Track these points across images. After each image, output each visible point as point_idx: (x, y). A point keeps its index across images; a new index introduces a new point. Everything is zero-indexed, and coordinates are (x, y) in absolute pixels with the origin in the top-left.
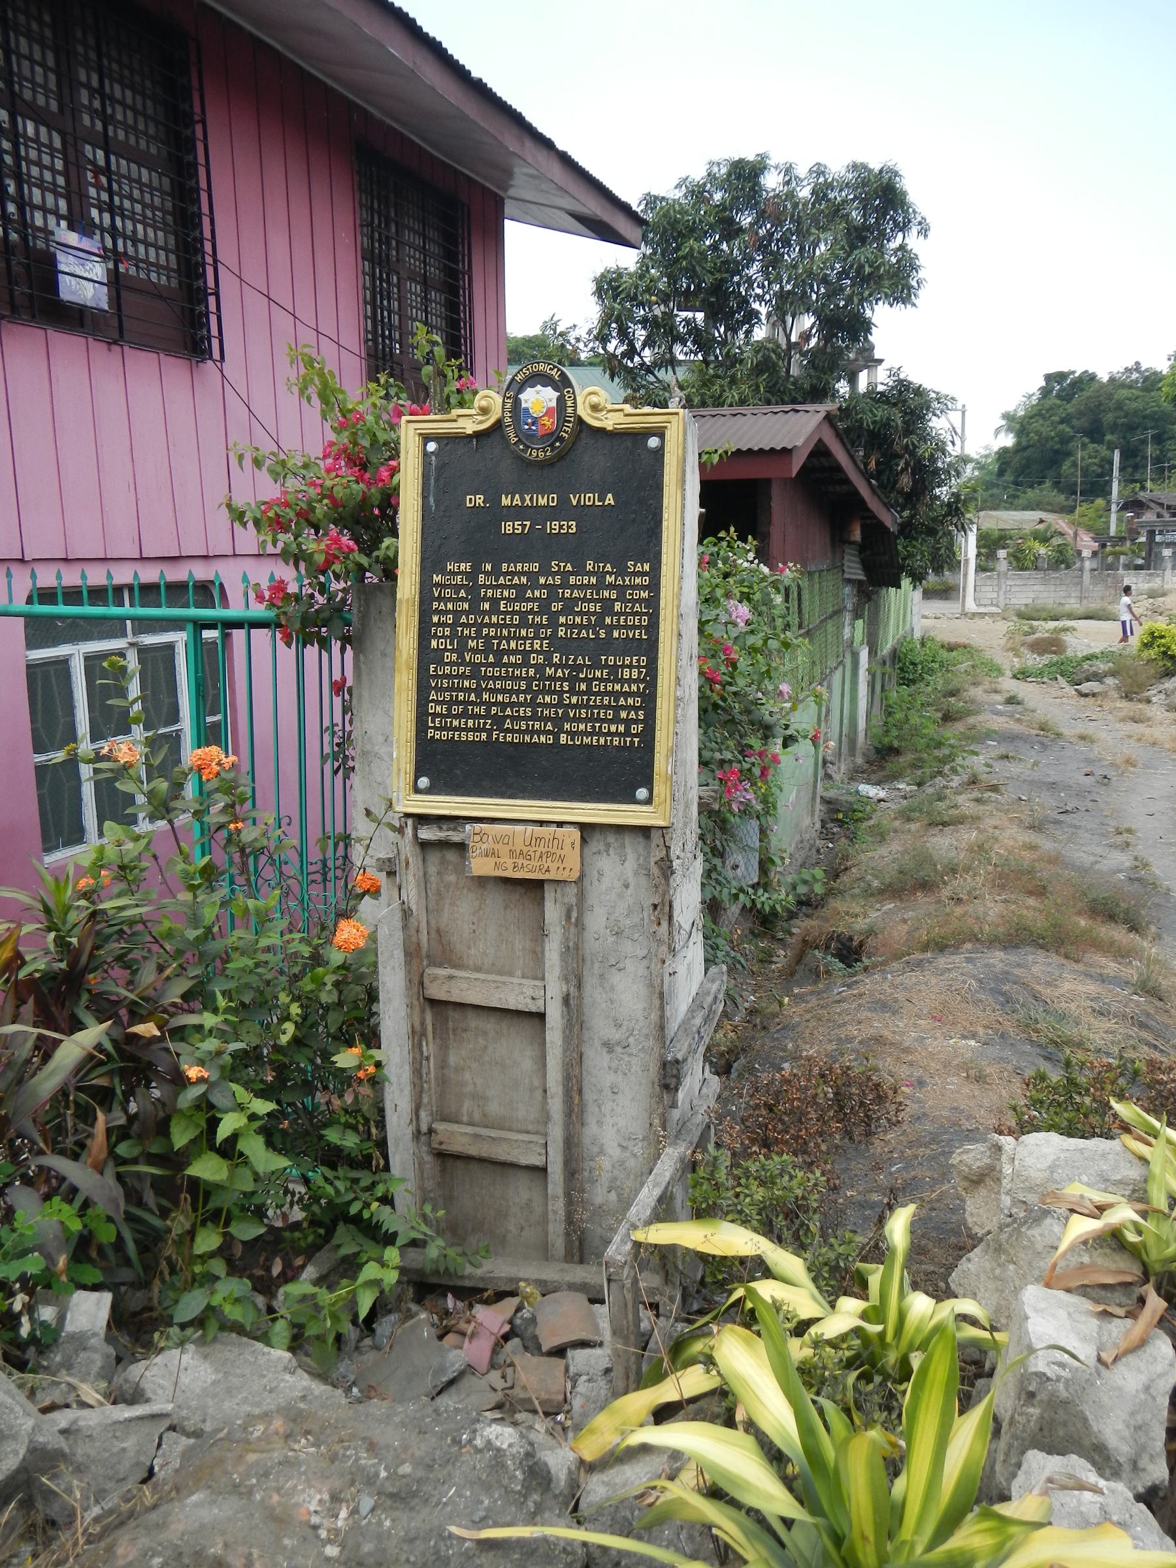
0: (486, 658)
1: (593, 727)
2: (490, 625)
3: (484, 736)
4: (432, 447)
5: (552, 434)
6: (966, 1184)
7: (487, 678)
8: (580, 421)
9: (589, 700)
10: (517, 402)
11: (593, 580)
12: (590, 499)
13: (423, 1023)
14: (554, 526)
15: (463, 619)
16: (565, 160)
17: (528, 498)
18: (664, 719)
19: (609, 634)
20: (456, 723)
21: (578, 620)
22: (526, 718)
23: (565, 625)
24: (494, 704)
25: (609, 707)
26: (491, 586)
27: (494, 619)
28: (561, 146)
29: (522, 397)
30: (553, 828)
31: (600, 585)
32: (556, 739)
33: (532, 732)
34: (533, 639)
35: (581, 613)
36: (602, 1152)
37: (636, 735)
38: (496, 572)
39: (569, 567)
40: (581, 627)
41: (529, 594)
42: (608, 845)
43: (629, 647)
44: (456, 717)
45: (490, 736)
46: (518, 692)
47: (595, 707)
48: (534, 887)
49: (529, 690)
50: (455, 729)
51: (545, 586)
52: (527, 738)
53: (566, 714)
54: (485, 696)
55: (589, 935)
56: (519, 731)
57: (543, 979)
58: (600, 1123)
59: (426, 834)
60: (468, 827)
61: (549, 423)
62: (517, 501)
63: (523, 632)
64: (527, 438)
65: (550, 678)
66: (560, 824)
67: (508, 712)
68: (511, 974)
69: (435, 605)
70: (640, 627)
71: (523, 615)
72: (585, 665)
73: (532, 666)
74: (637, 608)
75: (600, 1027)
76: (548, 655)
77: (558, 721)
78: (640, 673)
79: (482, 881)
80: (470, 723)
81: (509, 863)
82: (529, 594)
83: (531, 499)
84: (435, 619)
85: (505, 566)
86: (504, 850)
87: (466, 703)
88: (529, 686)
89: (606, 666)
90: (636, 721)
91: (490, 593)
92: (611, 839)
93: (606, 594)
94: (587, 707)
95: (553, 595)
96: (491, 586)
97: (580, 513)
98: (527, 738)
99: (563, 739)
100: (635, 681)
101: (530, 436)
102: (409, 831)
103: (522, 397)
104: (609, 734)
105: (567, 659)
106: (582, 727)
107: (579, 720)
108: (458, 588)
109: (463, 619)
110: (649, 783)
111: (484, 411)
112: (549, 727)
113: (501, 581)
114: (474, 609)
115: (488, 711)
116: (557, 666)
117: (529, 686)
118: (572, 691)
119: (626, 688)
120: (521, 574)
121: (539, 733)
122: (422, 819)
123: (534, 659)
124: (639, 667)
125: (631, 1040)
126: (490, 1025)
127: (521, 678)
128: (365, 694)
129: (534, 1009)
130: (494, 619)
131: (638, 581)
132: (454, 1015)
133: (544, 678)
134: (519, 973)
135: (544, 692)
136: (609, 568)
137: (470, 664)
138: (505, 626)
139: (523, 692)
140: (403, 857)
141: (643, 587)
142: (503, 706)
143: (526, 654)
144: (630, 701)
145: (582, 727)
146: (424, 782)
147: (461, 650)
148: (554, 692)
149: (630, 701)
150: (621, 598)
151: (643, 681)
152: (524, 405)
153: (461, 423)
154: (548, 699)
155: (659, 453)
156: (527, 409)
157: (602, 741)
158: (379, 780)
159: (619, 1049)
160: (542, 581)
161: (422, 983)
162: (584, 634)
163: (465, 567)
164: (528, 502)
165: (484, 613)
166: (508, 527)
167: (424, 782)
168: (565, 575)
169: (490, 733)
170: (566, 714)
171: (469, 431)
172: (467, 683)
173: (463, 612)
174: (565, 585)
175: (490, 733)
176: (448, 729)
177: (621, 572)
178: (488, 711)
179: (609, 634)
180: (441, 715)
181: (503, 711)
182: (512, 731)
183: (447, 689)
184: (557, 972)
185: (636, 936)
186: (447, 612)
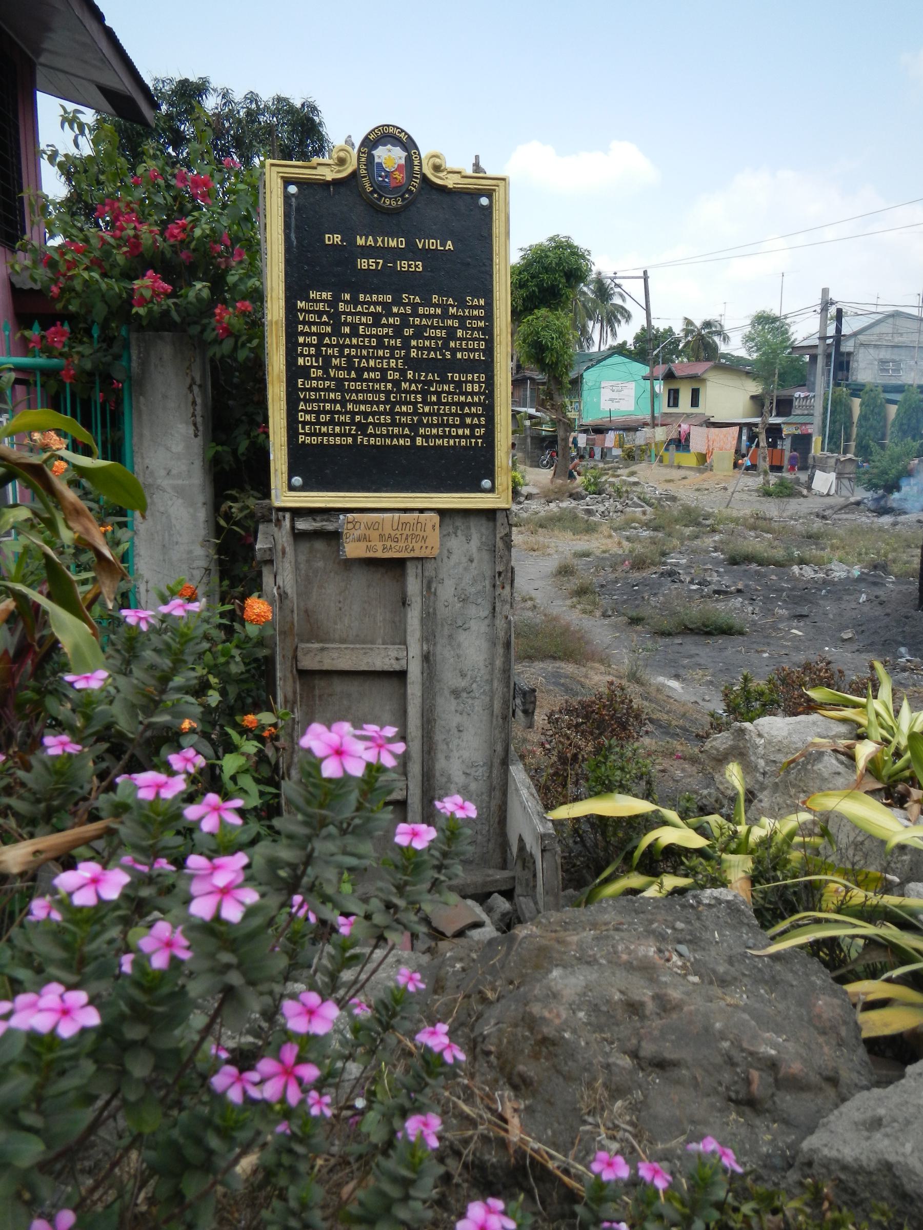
0: (349, 374)
1: (444, 431)
2: (350, 346)
3: (350, 440)
4: (293, 189)
6: (713, 763)
7: (350, 391)
8: (425, 178)
9: (439, 409)
10: (371, 158)
11: (439, 311)
13: (295, 693)
15: (327, 340)
16: (110, 34)
17: (380, 240)
20: (324, 429)
21: (427, 343)
22: (386, 425)
23: (418, 348)
24: (359, 413)
27: (354, 341)
28: (108, 23)
29: (375, 152)
30: (416, 515)
31: (445, 315)
32: (413, 440)
33: (392, 437)
35: (430, 338)
36: (449, 780)
37: (479, 437)
38: (355, 301)
39: (418, 300)
40: (429, 349)
41: (384, 321)
42: (457, 528)
43: (470, 366)
44: (324, 424)
45: (355, 440)
46: (378, 403)
48: (395, 567)
49: (387, 401)
50: (324, 435)
52: (388, 441)
54: (350, 407)
55: (440, 605)
56: (381, 436)
57: (405, 643)
58: (447, 758)
59: (302, 525)
60: (341, 517)
63: (381, 353)
64: (381, 189)
65: (406, 392)
66: (422, 511)
67: (370, 419)
68: (373, 642)
70: (478, 350)
71: (380, 338)
73: (389, 381)
74: (476, 335)
75: (450, 678)
76: (403, 373)
77: (414, 427)
78: (480, 387)
79: (350, 564)
80: (337, 429)
81: (379, 546)
82: (384, 321)
83: (383, 241)
84: (301, 340)
86: (374, 535)
88: (388, 398)
89: (453, 381)
90: (479, 426)
91: (349, 319)
92: (459, 522)
93: (450, 322)
94: (438, 415)
95: (405, 323)
97: (426, 255)
98: (388, 441)
99: (419, 441)
100: (476, 394)
102: (287, 523)
103: (375, 152)
104: (457, 436)
105: (420, 376)
106: (434, 431)
107: (431, 426)
108: (320, 314)
109: (327, 340)
110: (491, 476)
112: (407, 431)
113: (359, 309)
114: (336, 332)
115: (353, 419)
117: (388, 398)
118: (425, 402)
119: (469, 399)
120: (376, 304)
121: (398, 437)
122: (297, 513)
123: (390, 375)
124: (479, 382)
125: (474, 686)
126: (353, 687)
127: (379, 392)
128: (146, 432)
129: (397, 667)
130: (354, 341)
131: (476, 313)
132: (320, 684)
133: (400, 391)
134: (380, 641)
135: (401, 403)
136: (451, 301)
138: (364, 347)
139: (383, 403)
140: (279, 547)
141: (479, 318)
142: (366, 414)
143: (383, 371)
144: (473, 410)
145: (434, 431)
147: (326, 365)
148: (410, 403)
149: (473, 410)
150: (463, 326)
151: (482, 394)
152: (377, 160)
153: (321, 171)
154: (404, 409)
156: (380, 164)
158: (162, 509)
159: (464, 695)
160: (395, 310)
161: (295, 658)
162: (432, 355)
164: (380, 243)
165: (345, 336)
168: (415, 306)
169: (355, 437)
171: (329, 178)
172: (332, 396)
174: (415, 314)
175: (355, 437)
177: (462, 304)
178: (353, 419)
181: (366, 419)
182: (375, 436)
184: (418, 634)
185: (479, 601)
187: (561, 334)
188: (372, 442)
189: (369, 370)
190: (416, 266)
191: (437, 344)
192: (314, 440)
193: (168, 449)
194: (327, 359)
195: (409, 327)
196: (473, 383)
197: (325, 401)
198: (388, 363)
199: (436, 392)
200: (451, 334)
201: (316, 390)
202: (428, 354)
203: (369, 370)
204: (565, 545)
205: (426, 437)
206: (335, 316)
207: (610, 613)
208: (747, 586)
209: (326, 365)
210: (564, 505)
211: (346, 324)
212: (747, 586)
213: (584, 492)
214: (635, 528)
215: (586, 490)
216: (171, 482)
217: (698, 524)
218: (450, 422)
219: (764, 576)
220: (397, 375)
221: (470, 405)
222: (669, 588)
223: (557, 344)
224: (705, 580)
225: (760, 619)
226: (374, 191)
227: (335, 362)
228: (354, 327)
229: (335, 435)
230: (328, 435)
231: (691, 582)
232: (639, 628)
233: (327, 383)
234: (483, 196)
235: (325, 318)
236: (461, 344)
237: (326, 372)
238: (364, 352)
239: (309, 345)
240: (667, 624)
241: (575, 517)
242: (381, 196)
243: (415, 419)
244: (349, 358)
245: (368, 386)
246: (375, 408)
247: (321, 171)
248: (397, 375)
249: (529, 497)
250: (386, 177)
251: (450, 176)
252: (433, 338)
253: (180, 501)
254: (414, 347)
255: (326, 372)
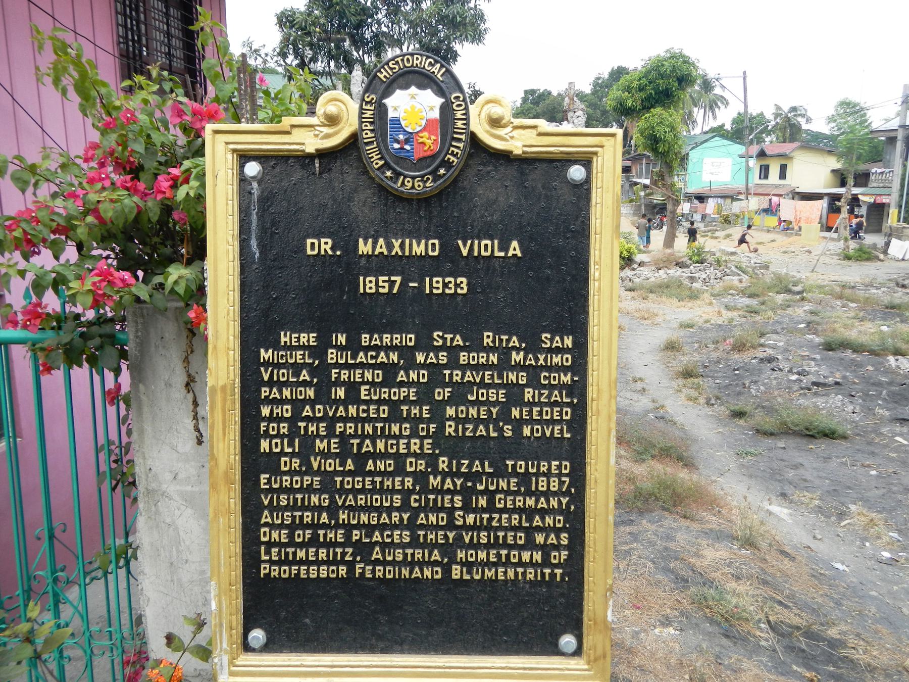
0: (343, 464)
1: (499, 556)
2: (345, 419)
4: (253, 169)
5: (433, 157)
7: (342, 491)
8: (473, 138)
9: (490, 519)
10: (381, 110)
11: (494, 358)
12: (486, 247)
14: (436, 284)
15: (307, 411)
17: (397, 244)
18: (600, 547)
19: (517, 430)
20: (301, 554)
22: (403, 546)
23: (457, 420)
24: (358, 526)
25: (519, 528)
26: (347, 366)
27: (352, 410)
29: (387, 101)
32: (447, 570)
33: (412, 564)
34: (408, 437)
35: (477, 403)
38: (354, 346)
39: (459, 341)
40: (478, 421)
43: (546, 448)
44: (301, 545)
46: (390, 510)
47: (500, 528)
50: (301, 562)
51: (424, 366)
52: (405, 572)
53: (459, 538)
54: (343, 516)
61: (430, 142)
62: (381, 247)
63: (395, 429)
64: (398, 163)
65: (435, 491)
67: (377, 537)
69: (264, 391)
71: (394, 405)
72: (484, 473)
73: (408, 474)
74: (556, 396)
76: (432, 460)
77: (448, 549)
78: (561, 483)
82: (401, 376)
83: (402, 246)
84: (265, 411)
85: (365, 337)
87: (315, 526)
89: (515, 474)
90: (557, 547)
93: (512, 377)
94: (489, 528)
96: (347, 366)
97: (474, 267)
98: (405, 572)
99: (456, 572)
100: (555, 494)
101: (402, 160)
103: (387, 101)
105: (459, 465)
106: (482, 555)
107: (475, 546)
108: (297, 368)
109: (307, 411)
110: (576, 627)
111: (332, 120)
112: (436, 556)
116: (445, 475)
118: (467, 508)
119: (542, 504)
120: (388, 349)
121: (421, 564)
124: (560, 475)
127: (393, 491)
128: (148, 428)
130: (352, 410)
131: (557, 359)
135: (426, 509)
137: (319, 472)
138: (368, 420)
139: (398, 509)
142: (370, 529)
143: (399, 458)
144: (549, 520)
145: (482, 555)
146: (258, 635)
147: (306, 451)
148: (442, 509)
149: (549, 520)
150: (534, 382)
151: (564, 494)
152: (391, 114)
153: (298, 136)
154: (432, 518)
155: (583, 190)
156: (396, 121)
157: (511, 573)
158: (168, 520)
160: (420, 358)
162: (481, 430)
163: (308, 338)
164: (397, 249)
165: (337, 402)
166: (369, 284)
167: (258, 635)
168: (453, 351)
170: (459, 538)
171: (310, 149)
172: (315, 499)
173: (305, 402)
174: (454, 363)
175: (351, 565)
176: (286, 562)
177: (533, 347)
179: (517, 430)
180: (279, 544)
181: (370, 535)
182: (384, 563)
183: (287, 508)
186: (281, 402)
187: (673, 128)
188: (379, 574)
189: (375, 456)
190: (457, 285)
191: (490, 413)
192: (285, 572)
193: (174, 449)
194: (308, 442)
195: (444, 385)
196: (552, 475)
197: (304, 508)
198: (408, 445)
199: (486, 491)
200: (514, 394)
201: (290, 490)
202: (475, 430)
203: (375, 456)
204: (673, 314)
205: (469, 565)
206: (321, 371)
207: (713, 401)
208: (844, 377)
209: (306, 451)
210: (672, 272)
211: (338, 383)
212: (844, 377)
213: (689, 262)
214: (732, 295)
215: (690, 259)
216: (178, 487)
217: (789, 291)
218: (510, 540)
219: (859, 365)
220: (421, 465)
221: (543, 513)
222: (768, 376)
223: (669, 137)
224: (804, 370)
225: (861, 420)
226: (386, 165)
227: (321, 445)
228: (352, 388)
229: (318, 563)
230: (308, 563)
231: (790, 371)
232: (742, 422)
233: (307, 480)
234: (576, 162)
235: (305, 375)
236: (530, 412)
237: (306, 462)
238: (369, 429)
239: (280, 419)
240: (769, 423)
241: (680, 285)
242: (397, 174)
243: (451, 535)
244: (344, 438)
245: (373, 482)
246: (385, 519)
247: (298, 136)
248: (421, 465)
249: (641, 264)
250: (407, 141)
251: (516, 133)
252: (483, 403)
253: (189, 511)
254: (450, 418)
255: (306, 462)
